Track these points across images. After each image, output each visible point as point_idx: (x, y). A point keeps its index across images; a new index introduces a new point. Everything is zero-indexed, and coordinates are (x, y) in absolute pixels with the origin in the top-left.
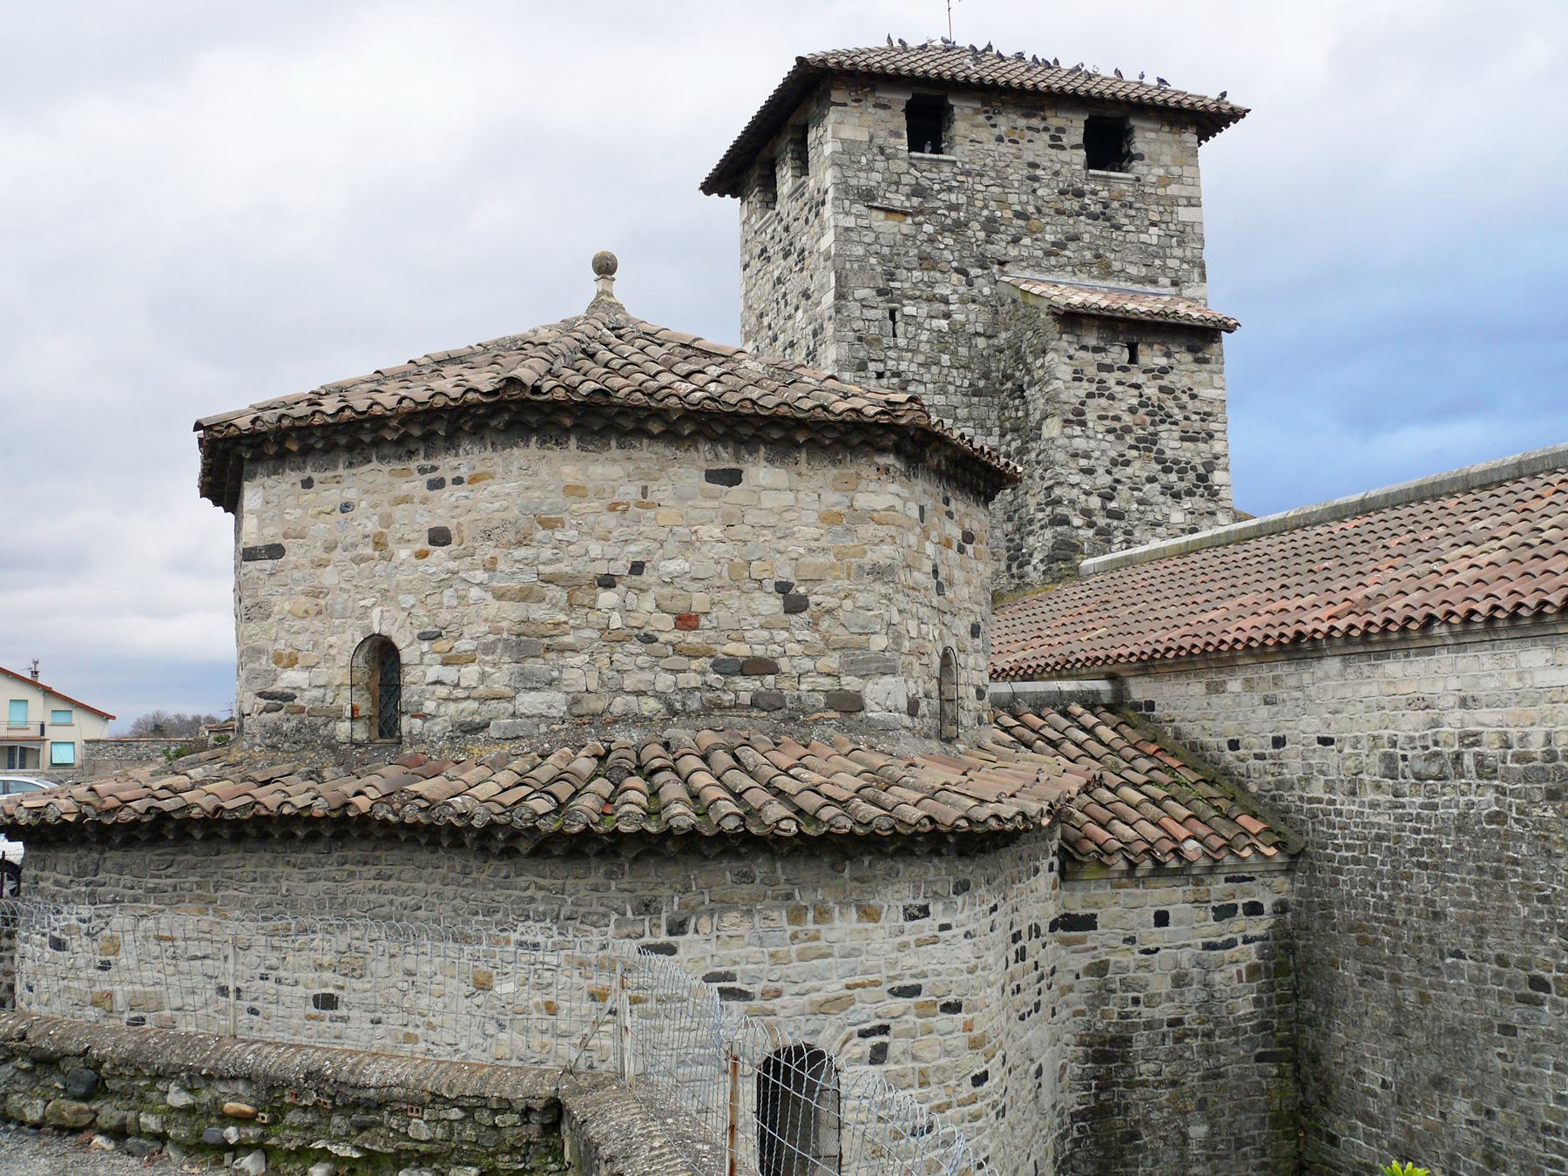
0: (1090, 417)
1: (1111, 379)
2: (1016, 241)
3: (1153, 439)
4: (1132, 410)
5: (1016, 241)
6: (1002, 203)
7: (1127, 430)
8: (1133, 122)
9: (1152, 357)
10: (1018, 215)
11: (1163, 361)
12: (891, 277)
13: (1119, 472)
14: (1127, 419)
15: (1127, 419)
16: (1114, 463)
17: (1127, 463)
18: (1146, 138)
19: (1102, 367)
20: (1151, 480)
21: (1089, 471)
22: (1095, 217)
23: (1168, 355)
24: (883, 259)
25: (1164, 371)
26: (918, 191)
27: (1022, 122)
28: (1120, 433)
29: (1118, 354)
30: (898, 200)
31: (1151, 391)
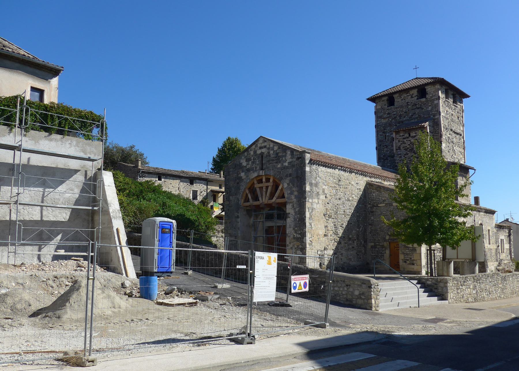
0: (401, 147)
1: (405, 140)
2: (405, 117)
3: (413, 149)
4: (409, 145)
5: (405, 117)
6: (402, 111)
7: (408, 148)
8: (426, 87)
9: (413, 134)
10: (405, 112)
11: (415, 135)
12: (385, 129)
13: (406, 156)
14: (408, 146)
15: (408, 146)
16: (405, 155)
17: (408, 154)
18: (429, 89)
19: (404, 139)
20: (412, 156)
21: (401, 157)
22: (418, 108)
23: (416, 133)
24: (384, 127)
25: (415, 136)
26: (389, 114)
27: (406, 95)
28: (406, 150)
29: (407, 135)
30: (385, 116)
31: (412, 140)
